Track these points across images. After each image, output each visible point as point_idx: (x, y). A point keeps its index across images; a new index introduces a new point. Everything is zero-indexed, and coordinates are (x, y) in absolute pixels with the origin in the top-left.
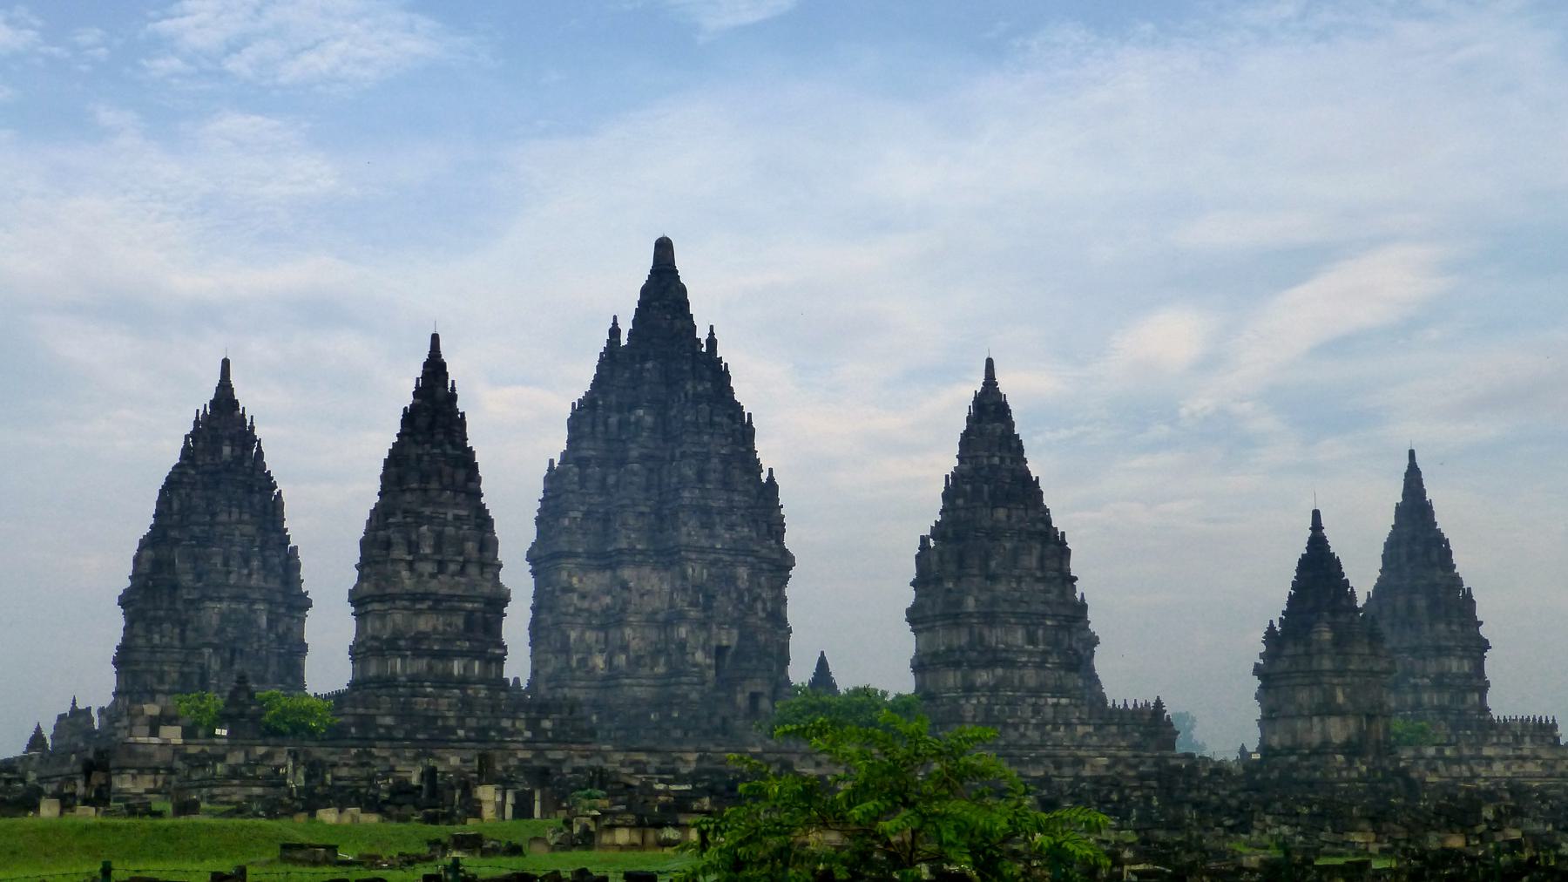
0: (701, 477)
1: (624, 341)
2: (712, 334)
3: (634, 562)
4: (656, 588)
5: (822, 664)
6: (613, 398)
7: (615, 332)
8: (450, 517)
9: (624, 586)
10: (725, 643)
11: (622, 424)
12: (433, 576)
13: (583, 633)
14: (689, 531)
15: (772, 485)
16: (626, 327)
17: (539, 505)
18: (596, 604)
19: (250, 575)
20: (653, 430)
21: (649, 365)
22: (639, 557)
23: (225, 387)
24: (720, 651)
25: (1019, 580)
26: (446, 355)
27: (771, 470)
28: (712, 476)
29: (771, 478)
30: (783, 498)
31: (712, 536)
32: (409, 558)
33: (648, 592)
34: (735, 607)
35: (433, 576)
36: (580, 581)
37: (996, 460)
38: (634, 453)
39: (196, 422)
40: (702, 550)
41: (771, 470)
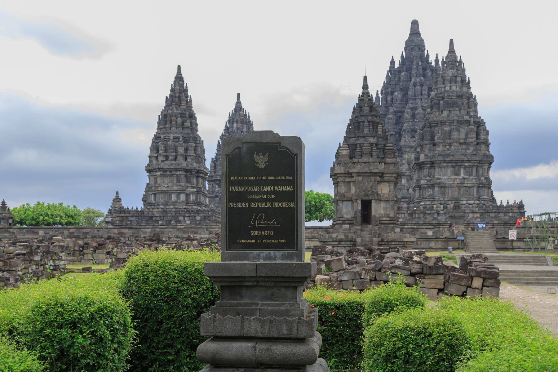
0: (413, 116)
1: (397, 65)
7: (393, 62)
8: (171, 138)
11: (392, 99)
12: (163, 161)
20: (402, 100)
21: (403, 74)
23: (238, 103)
25: (450, 144)
26: (184, 74)
28: (418, 116)
32: (156, 155)
35: (163, 161)
37: (447, 88)
39: (229, 117)
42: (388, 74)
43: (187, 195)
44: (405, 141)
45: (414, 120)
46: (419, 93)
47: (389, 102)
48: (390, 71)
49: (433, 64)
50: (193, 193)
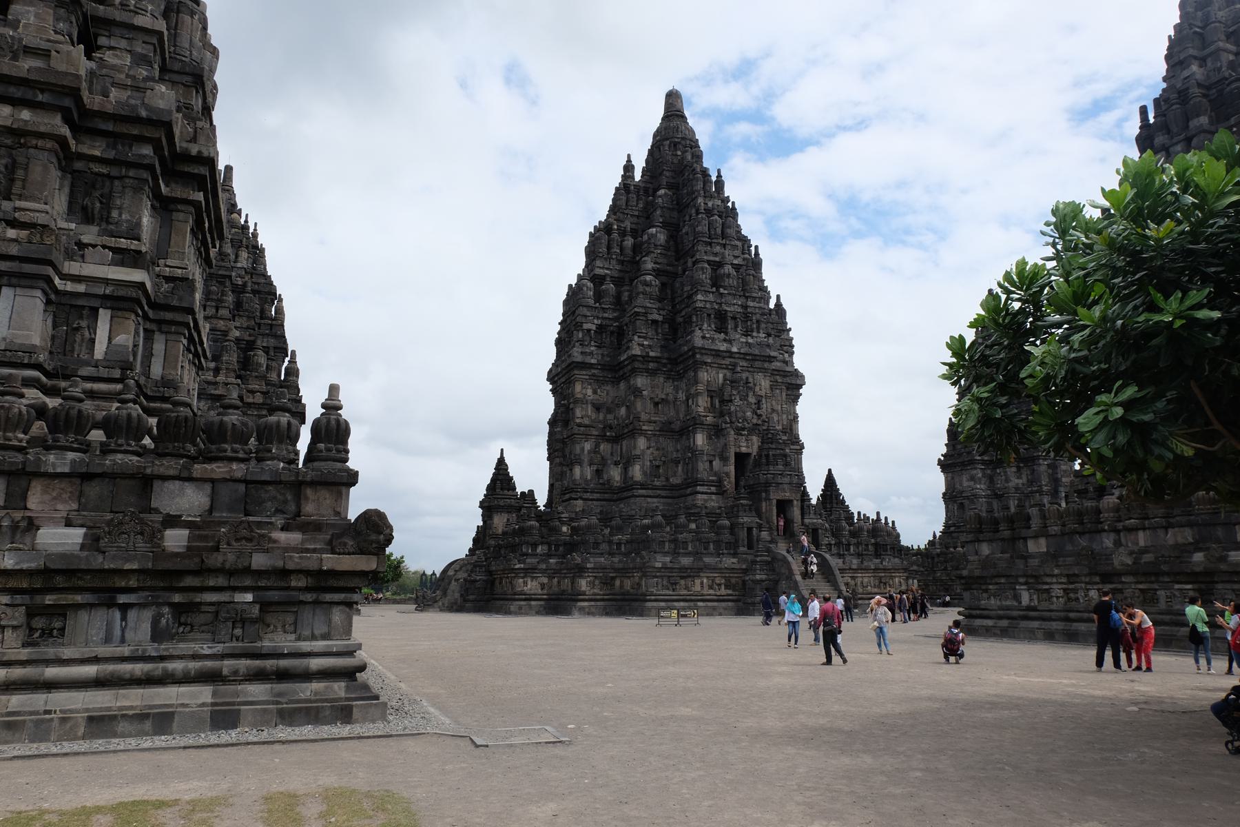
0: (716, 282)
1: (638, 176)
2: (719, 176)
3: (647, 370)
4: (671, 397)
5: (830, 481)
6: (627, 224)
7: (629, 168)
9: (637, 392)
10: (744, 450)
13: (597, 445)
14: (702, 336)
15: (780, 310)
16: (639, 164)
17: (558, 328)
18: (610, 417)
19: (217, 371)
20: (666, 248)
21: (662, 192)
22: (651, 365)
24: (741, 458)
27: (778, 297)
28: (727, 282)
29: (779, 305)
30: (790, 321)
31: (730, 342)
33: (664, 401)
34: (754, 412)
36: (595, 392)
38: (650, 266)
40: (717, 354)
41: (778, 297)
43: (71, 312)
44: (704, 337)
45: (718, 290)
46: (719, 231)
47: (629, 252)
50: (122, 301)
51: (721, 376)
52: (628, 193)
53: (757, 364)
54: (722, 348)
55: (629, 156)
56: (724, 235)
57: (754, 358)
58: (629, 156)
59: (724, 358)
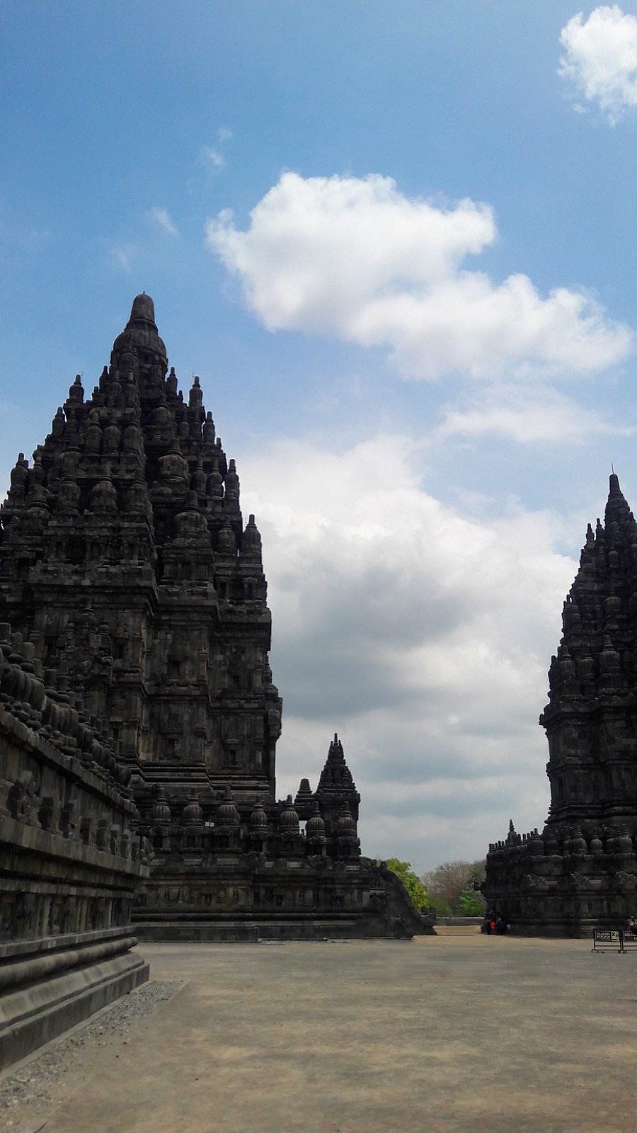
1: (88, 397)
2: (197, 385)
7: (77, 390)
27: (252, 517)
41: (252, 517)
42: (59, 415)
44: (45, 571)
45: (81, 512)
48: (67, 407)
49: (186, 400)
51: (66, 617)
52: (74, 417)
53: (123, 598)
54: (67, 583)
55: (78, 377)
56: (121, 447)
57: (118, 591)
58: (78, 377)
59: (74, 595)
